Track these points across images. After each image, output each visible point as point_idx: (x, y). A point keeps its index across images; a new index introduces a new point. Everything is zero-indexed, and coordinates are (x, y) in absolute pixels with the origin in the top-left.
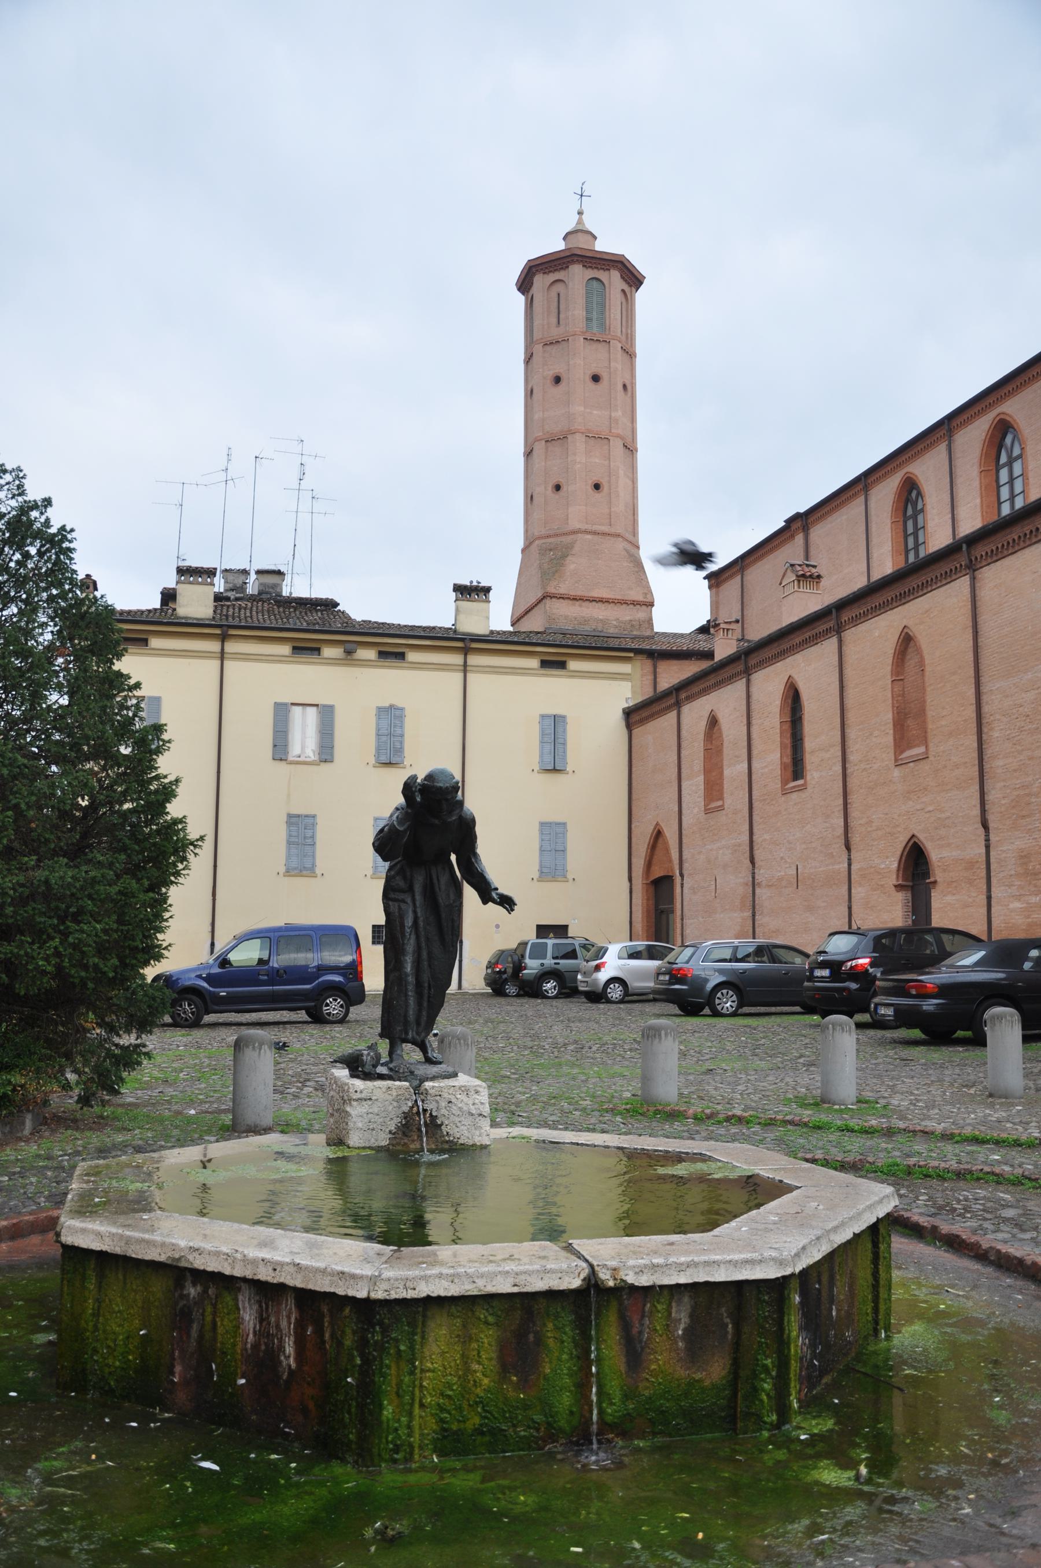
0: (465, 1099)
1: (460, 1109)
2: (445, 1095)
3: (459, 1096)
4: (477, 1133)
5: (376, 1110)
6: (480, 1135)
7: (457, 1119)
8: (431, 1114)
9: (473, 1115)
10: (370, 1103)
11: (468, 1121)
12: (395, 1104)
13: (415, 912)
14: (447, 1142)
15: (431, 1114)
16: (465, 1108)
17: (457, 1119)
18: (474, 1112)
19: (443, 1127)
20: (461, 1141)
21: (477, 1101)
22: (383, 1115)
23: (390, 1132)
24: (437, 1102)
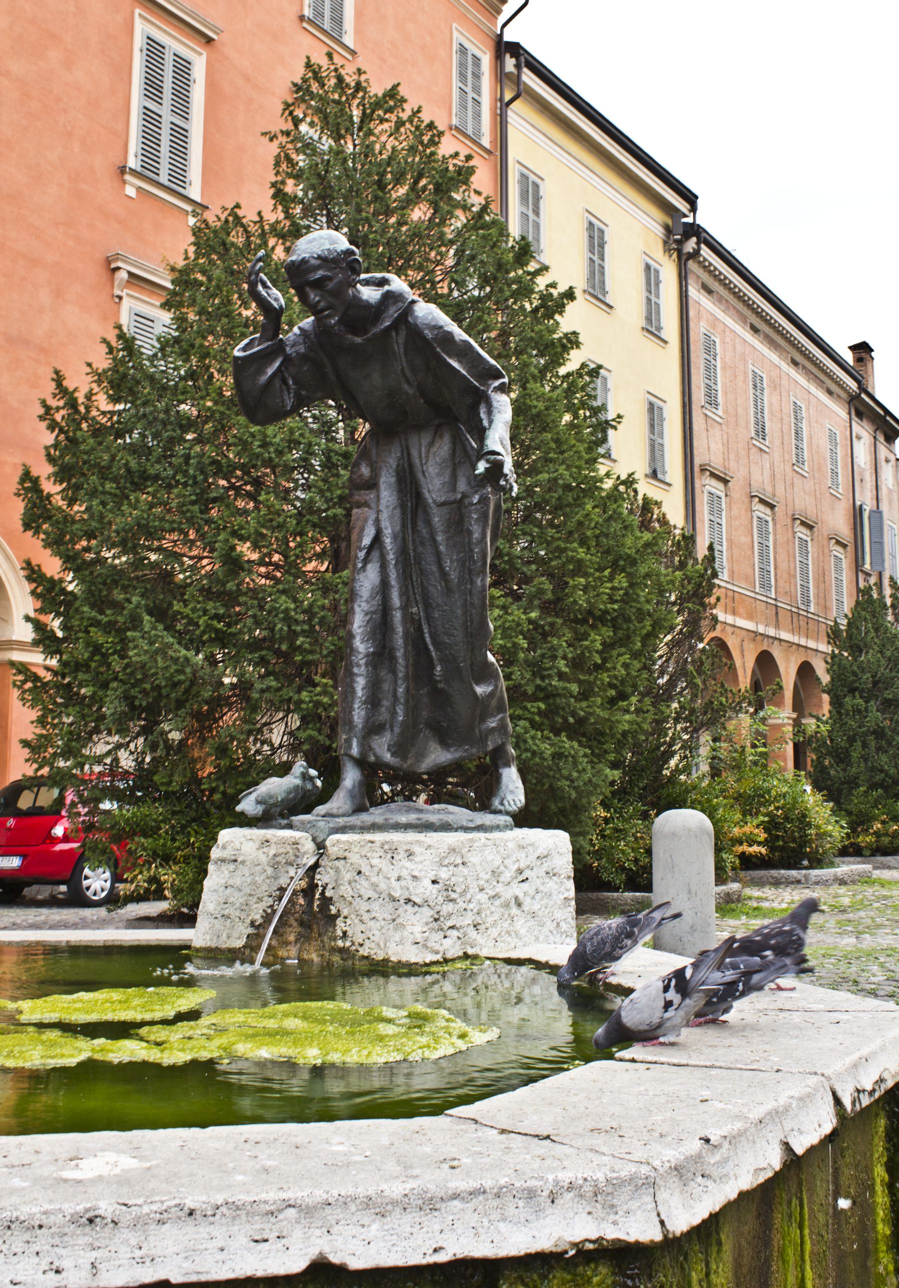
0: (384, 864)
1: (375, 886)
2: (354, 858)
3: (375, 861)
4: (397, 937)
5: (238, 881)
6: (401, 943)
7: (363, 906)
8: (323, 893)
9: (394, 900)
10: (232, 867)
11: (381, 910)
12: (270, 871)
13: (377, 521)
14: (342, 950)
15: (323, 893)
16: (383, 886)
17: (363, 906)
18: (396, 895)
19: (339, 922)
20: (363, 952)
21: (405, 873)
22: (247, 890)
23: (252, 924)
24: (337, 870)
